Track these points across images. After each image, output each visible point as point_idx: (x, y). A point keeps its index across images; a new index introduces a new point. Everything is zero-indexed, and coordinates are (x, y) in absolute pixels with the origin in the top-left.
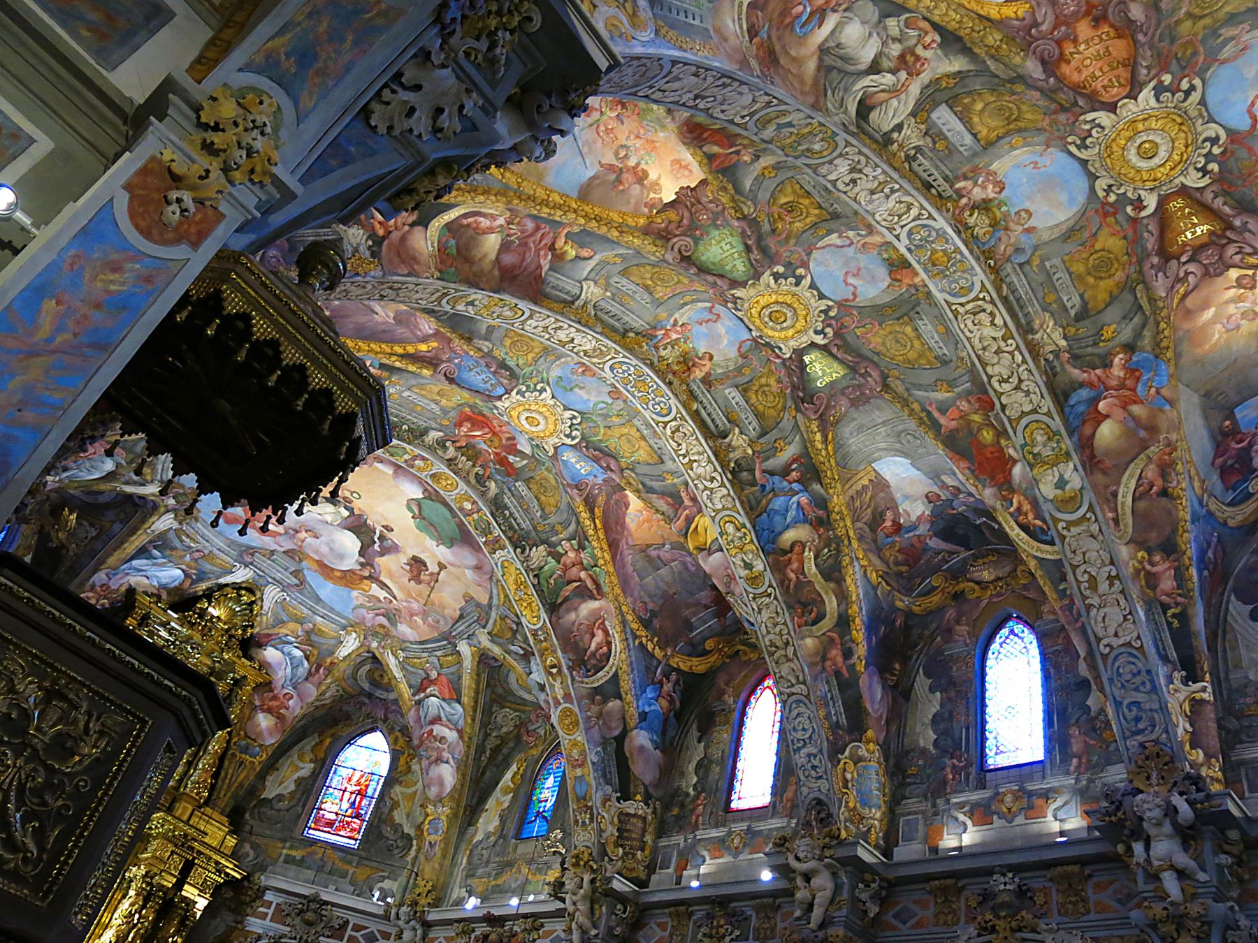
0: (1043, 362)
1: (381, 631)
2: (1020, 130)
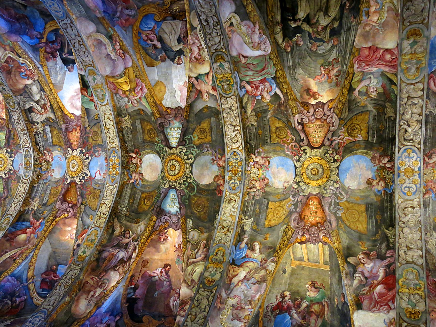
0: (27, 208)
2: (60, 146)
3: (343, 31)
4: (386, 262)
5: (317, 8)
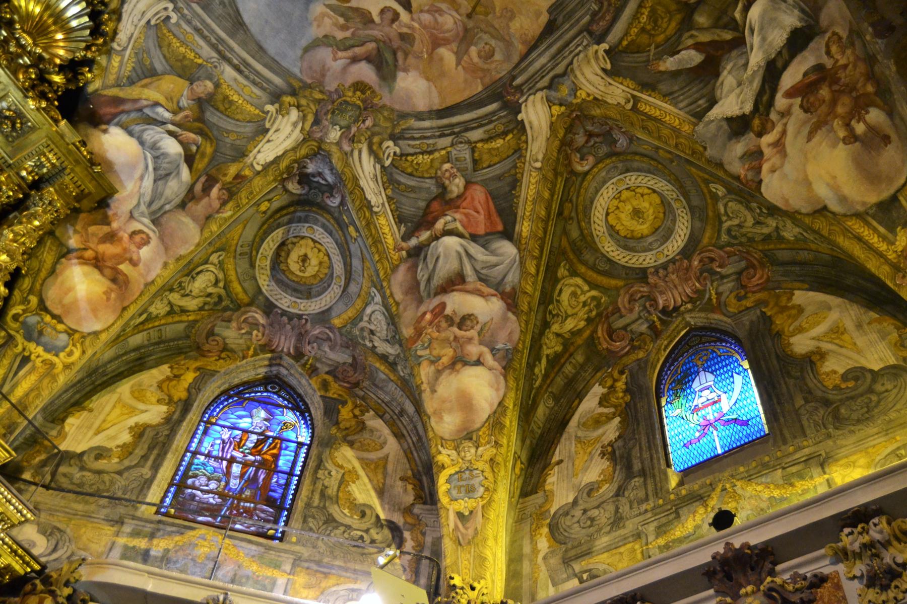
1: (355, 98)
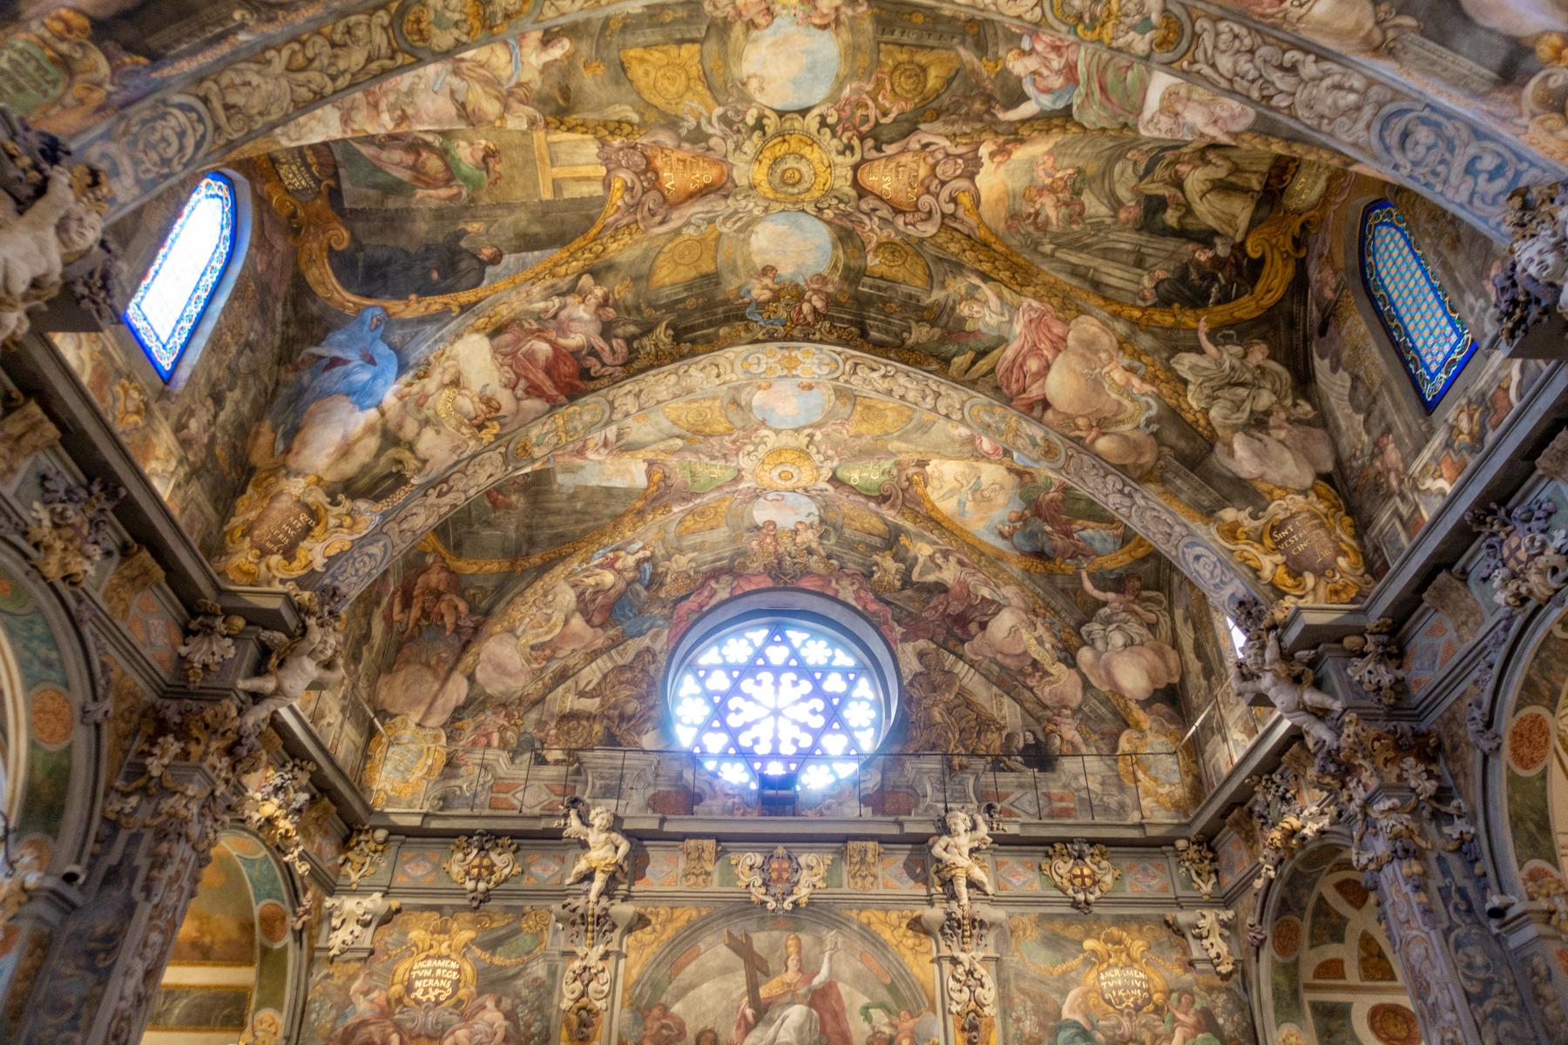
3: (1143, 238)
4: (599, 343)
5: (1245, 164)
